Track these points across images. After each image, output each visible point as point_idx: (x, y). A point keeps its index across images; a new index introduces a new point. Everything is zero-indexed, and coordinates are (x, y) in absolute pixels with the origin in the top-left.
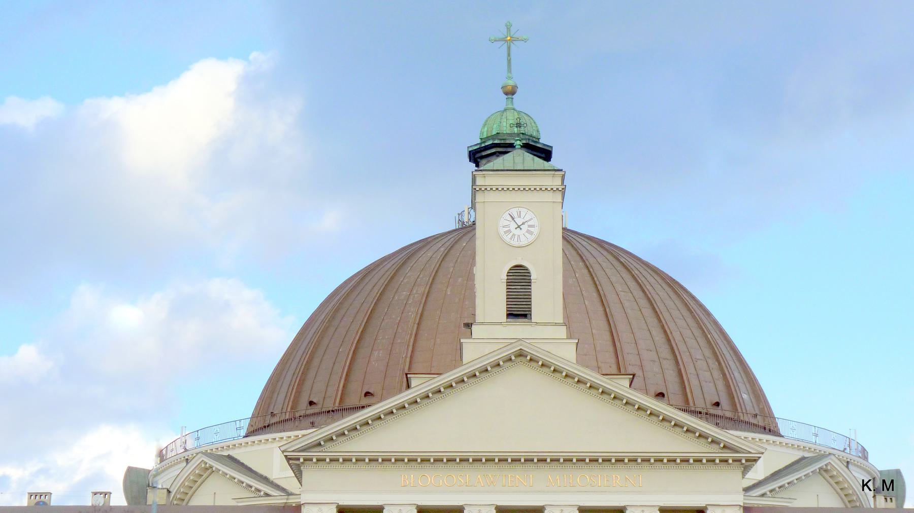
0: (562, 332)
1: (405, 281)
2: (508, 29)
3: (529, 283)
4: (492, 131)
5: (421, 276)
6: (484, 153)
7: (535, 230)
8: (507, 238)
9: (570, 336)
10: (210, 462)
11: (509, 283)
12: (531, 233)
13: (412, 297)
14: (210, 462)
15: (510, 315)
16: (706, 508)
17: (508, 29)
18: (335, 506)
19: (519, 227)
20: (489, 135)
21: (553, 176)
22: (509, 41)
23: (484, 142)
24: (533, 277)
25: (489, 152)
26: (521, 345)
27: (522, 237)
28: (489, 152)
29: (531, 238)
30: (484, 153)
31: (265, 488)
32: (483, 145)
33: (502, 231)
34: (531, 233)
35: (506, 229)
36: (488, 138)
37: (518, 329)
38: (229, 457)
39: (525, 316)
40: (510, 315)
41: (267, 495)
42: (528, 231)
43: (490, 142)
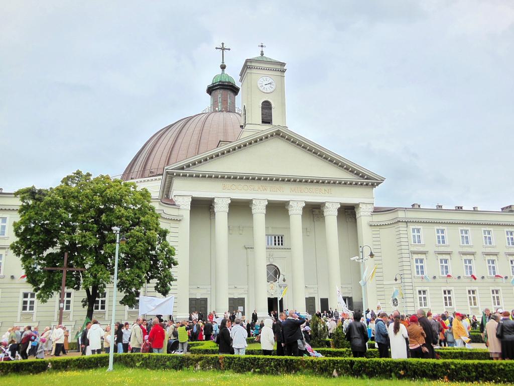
2: (223, 45)
3: (271, 109)
7: (274, 87)
8: (262, 90)
12: (272, 88)
15: (264, 122)
17: (223, 45)
22: (223, 49)
26: (279, 128)
27: (268, 89)
29: (272, 90)
33: (259, 86)
34: (272, 88)
37: (266, 127)
39: (269, 123)
40: (264, 122)
42: (270, 87)
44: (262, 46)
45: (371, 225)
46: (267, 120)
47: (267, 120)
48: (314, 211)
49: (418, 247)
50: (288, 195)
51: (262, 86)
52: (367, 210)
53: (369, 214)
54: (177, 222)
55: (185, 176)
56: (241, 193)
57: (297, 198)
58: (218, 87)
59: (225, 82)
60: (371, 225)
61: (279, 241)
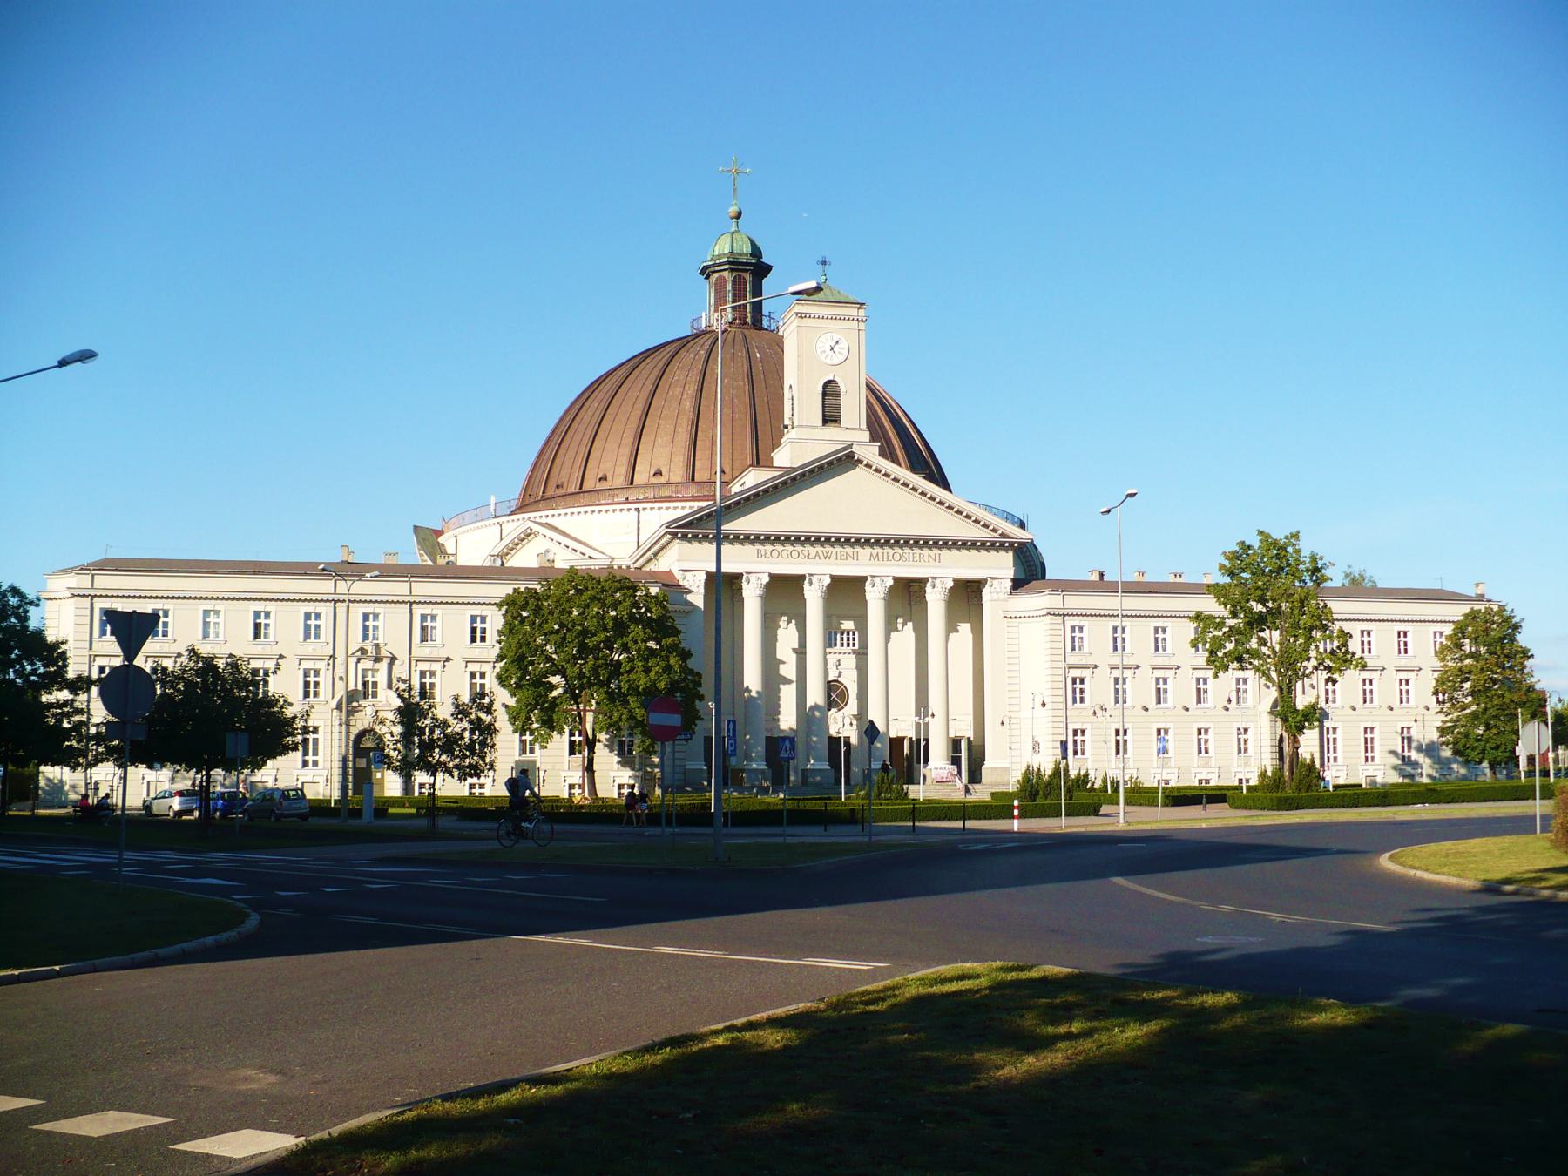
0: (866, 435)
1: (676, 378)
3: (839, 395)
4: (723, 250)
5: (690, 375)
6: (717, 268)
8: (822, 357)
9: (873, 439)
10: (536, 528)
11: (824, 394)
13: (685, 393)
14: (536, 528)
16: (986, 581)
18: (704, 572)
19: (832, 349)
20: (721, 252)
21: (859, 308)
23: (719, 259)
24: (843, 390)
25: (722, 268)
28: (722, 268)
30: (717, 268)
31: (589, 552)
32: (718, 262)
35: (821, 350)
36: (720, 257)
37: (831, 432)
38: (546, 523)
39: (836, 421)
41: (591, 558)
43: (725, 260)
44: (824, 263)
45: (1005, 617)
46: (831, 417)
47: (831, 417)
48: (908, 594)
49: (1080, 658)
50: (866, 565)
51: (825, 352)
52: (998, 590)
53: (1002, 597)
54: (684, 614)
55: (695, 536)
56: (787, 563)
57: (880, 570)
58: (727, 267)
59: (741, 254)
60: (1005, 617)
61: (848, 639)
